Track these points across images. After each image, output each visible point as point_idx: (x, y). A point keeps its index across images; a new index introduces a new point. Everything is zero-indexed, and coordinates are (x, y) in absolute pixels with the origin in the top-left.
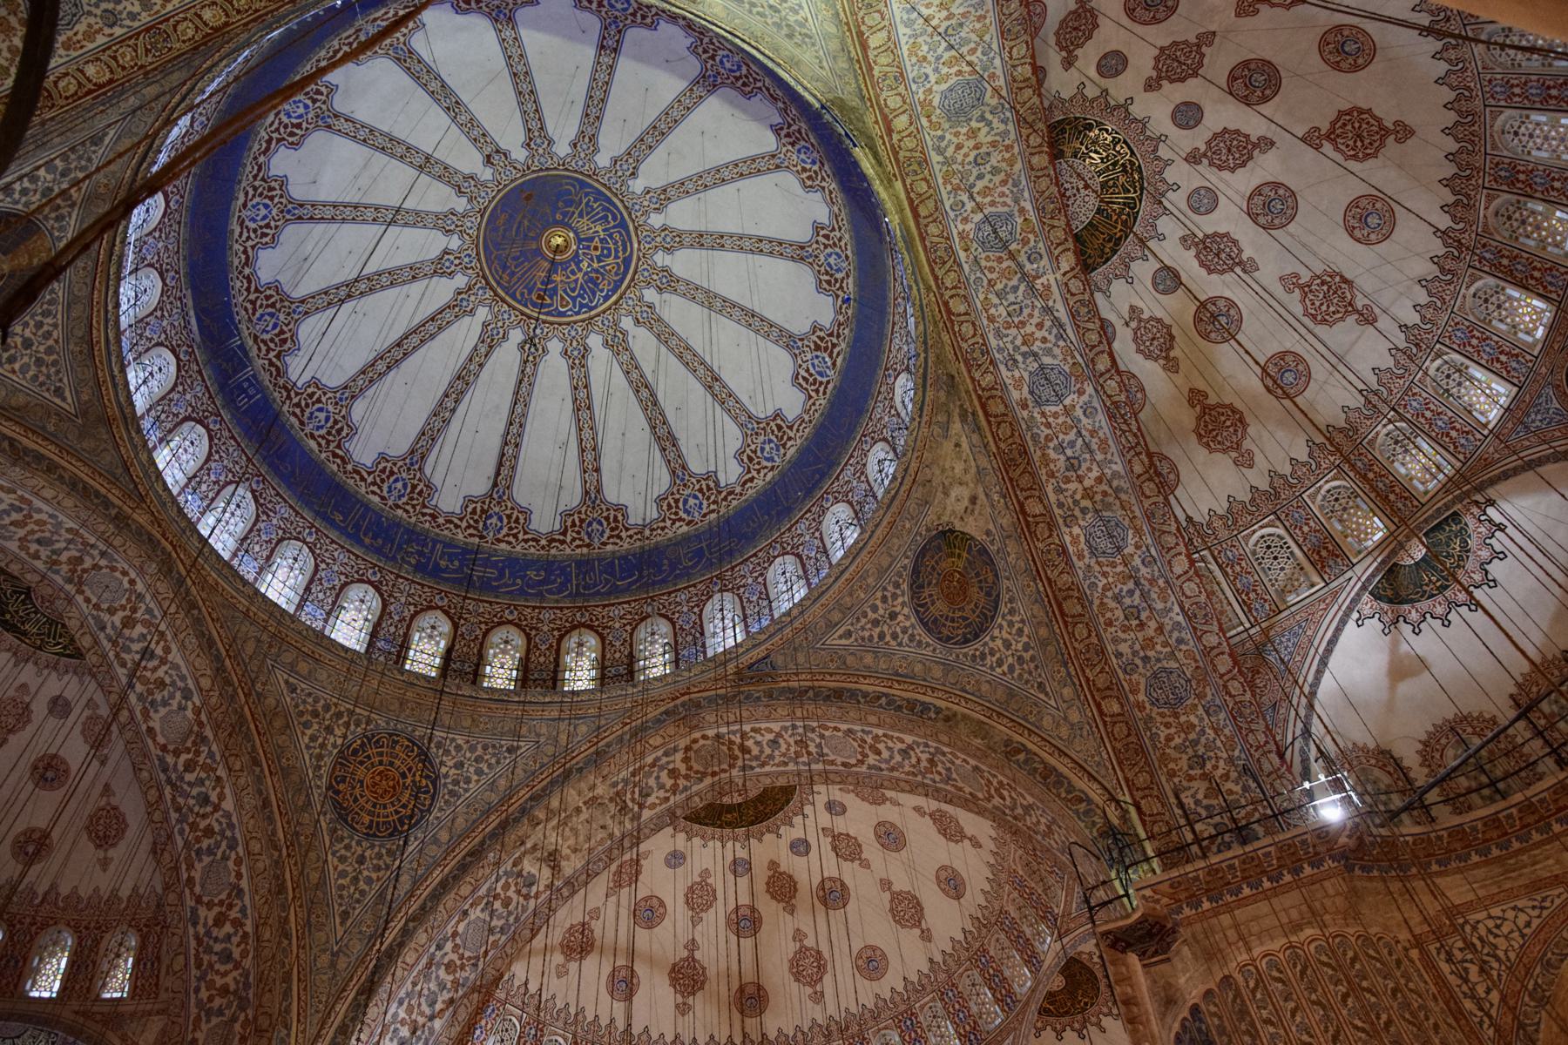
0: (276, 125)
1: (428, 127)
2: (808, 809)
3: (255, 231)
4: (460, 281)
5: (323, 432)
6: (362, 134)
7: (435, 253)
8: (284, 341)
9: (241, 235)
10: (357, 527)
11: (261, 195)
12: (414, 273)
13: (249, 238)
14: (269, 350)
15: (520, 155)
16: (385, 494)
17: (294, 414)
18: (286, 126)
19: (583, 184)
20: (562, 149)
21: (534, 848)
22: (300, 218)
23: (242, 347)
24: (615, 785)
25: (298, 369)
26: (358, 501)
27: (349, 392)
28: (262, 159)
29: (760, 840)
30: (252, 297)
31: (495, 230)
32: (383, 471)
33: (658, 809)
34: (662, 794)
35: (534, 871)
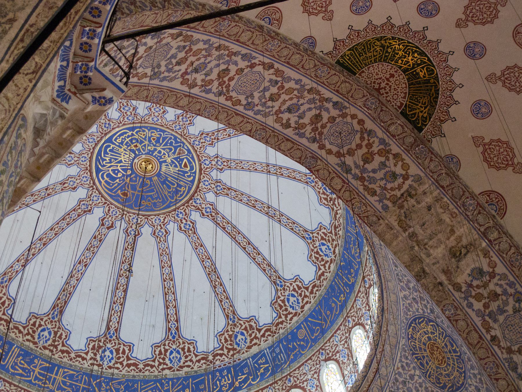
0: (118, 365)
1: (101, 272)
2: (378, 21)
3: (186, 357)
4: (195, 216)
5: (300, 301)
6: (117, 308)
7: (182, 236)
8: (251, 326)
9: (189, 366)
10: (346, 284)
11: (164, 359)
12: (198, 246)
13: (191, 360)
14: (256, 337)
15: (98, 212)
16: (329, 259)
17: (291, 319)
18: (119, 358)
19: (98, 171)
20: (82, 193)
21: (446, 272)
22: (177, 329)
23: (253, 357)
24: (386, 208)
25: (266, 316)
26: (334, 280)
27: (276, 280)
28: (141, 366)
29: (438, 42)
30: (226, 351)
31: (155, 204)
32: (317, 259)
33: (408, 160)
34: (391, 162)
35: (468, 271)
